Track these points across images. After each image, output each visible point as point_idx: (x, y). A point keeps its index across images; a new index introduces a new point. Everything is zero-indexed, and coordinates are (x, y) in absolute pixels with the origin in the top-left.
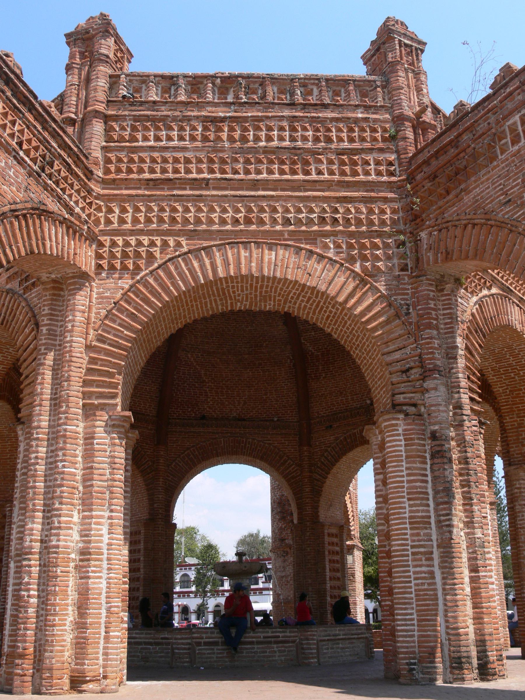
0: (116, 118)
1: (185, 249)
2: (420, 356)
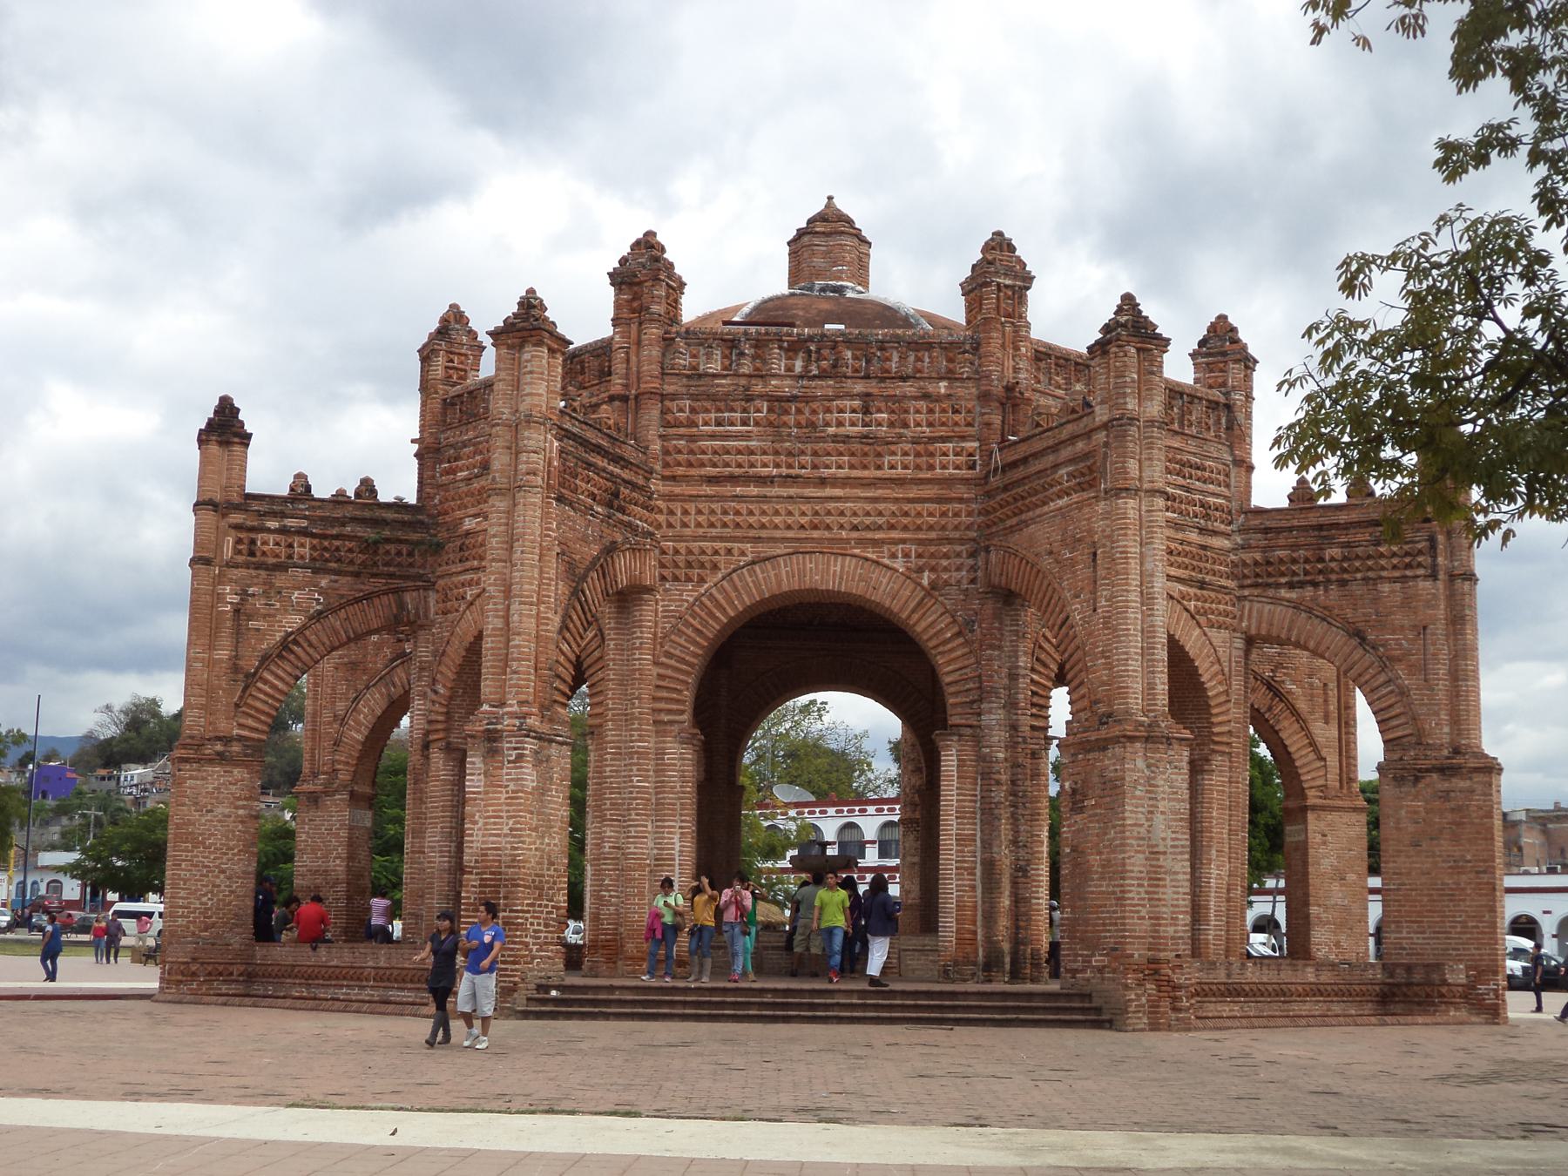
0: (673, 397)
1: (749, 558)
2: (980, 676)
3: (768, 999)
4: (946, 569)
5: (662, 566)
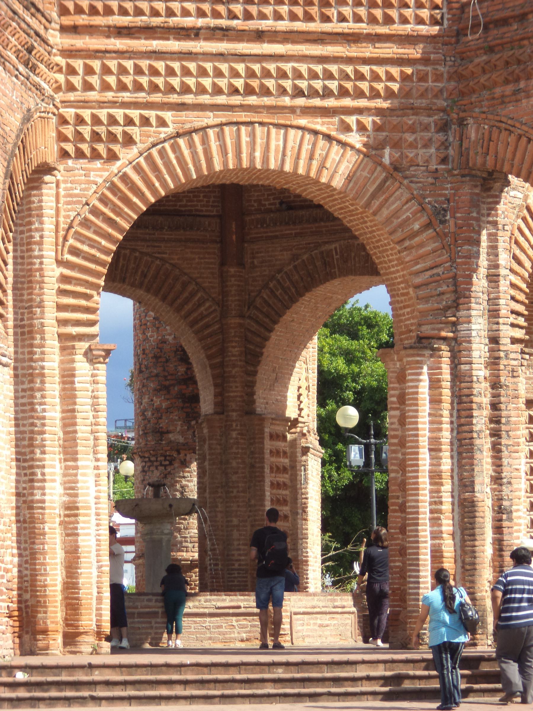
2: (455, 277)
3: (280, 673)
4: (412, 146)
5: (62, 138)
